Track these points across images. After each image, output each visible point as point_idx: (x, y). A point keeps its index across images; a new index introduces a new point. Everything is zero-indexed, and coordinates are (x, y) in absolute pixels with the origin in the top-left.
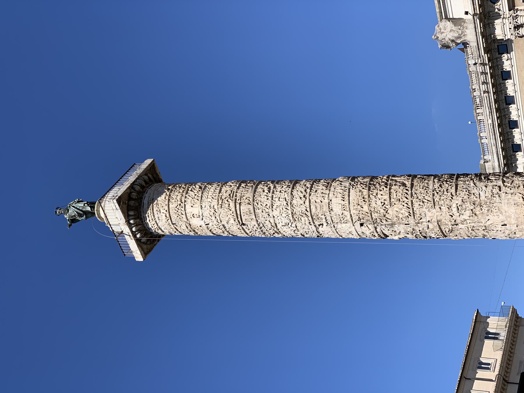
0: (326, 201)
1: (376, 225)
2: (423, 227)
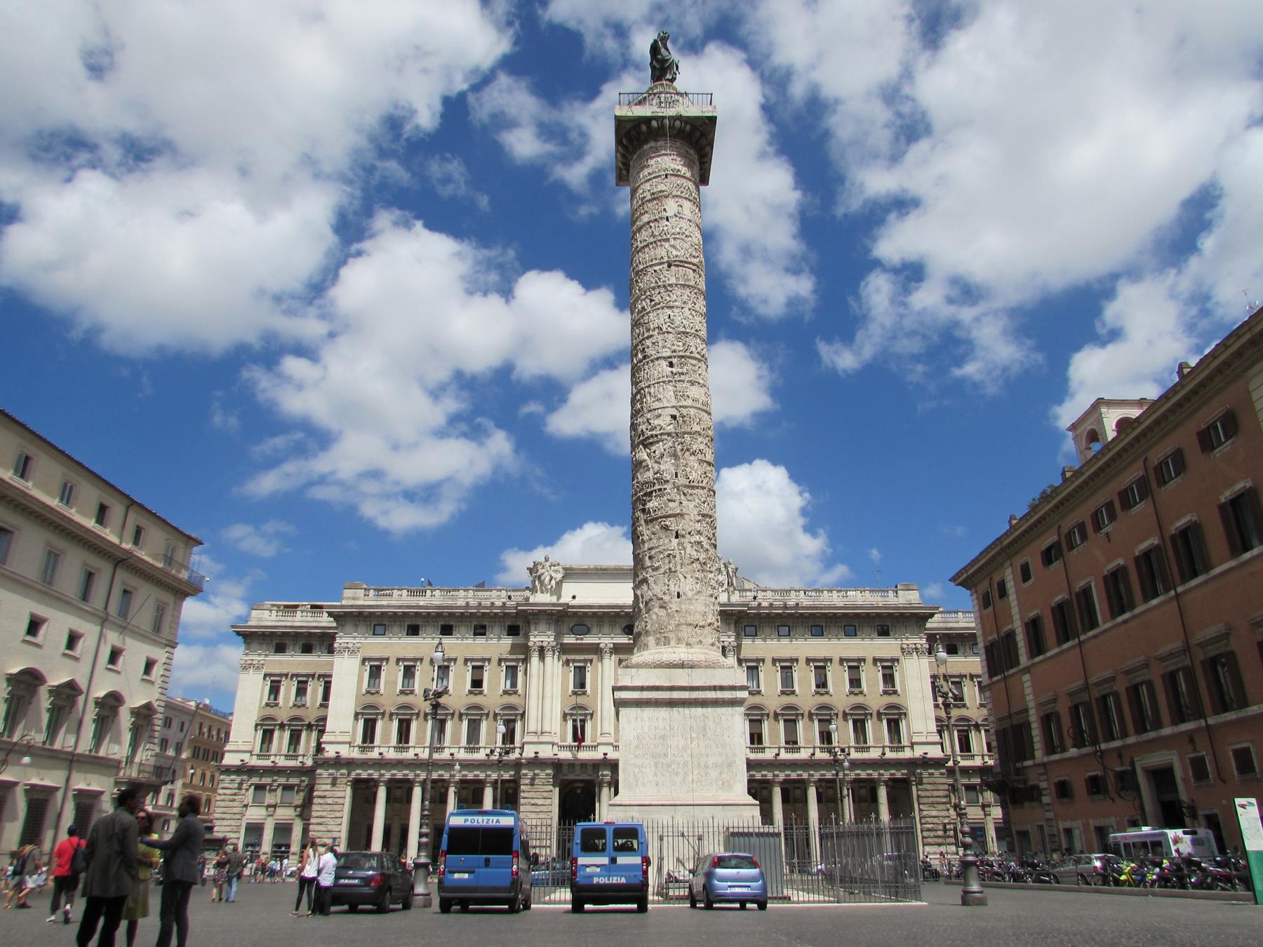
0: (701, 381)
1: (674, 435)
2: (672, 495)
